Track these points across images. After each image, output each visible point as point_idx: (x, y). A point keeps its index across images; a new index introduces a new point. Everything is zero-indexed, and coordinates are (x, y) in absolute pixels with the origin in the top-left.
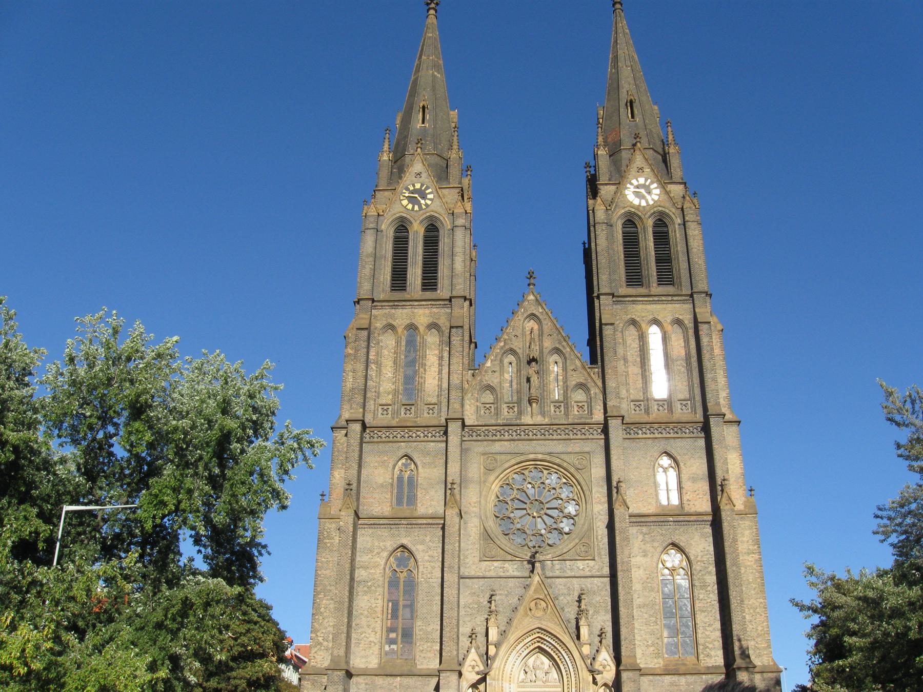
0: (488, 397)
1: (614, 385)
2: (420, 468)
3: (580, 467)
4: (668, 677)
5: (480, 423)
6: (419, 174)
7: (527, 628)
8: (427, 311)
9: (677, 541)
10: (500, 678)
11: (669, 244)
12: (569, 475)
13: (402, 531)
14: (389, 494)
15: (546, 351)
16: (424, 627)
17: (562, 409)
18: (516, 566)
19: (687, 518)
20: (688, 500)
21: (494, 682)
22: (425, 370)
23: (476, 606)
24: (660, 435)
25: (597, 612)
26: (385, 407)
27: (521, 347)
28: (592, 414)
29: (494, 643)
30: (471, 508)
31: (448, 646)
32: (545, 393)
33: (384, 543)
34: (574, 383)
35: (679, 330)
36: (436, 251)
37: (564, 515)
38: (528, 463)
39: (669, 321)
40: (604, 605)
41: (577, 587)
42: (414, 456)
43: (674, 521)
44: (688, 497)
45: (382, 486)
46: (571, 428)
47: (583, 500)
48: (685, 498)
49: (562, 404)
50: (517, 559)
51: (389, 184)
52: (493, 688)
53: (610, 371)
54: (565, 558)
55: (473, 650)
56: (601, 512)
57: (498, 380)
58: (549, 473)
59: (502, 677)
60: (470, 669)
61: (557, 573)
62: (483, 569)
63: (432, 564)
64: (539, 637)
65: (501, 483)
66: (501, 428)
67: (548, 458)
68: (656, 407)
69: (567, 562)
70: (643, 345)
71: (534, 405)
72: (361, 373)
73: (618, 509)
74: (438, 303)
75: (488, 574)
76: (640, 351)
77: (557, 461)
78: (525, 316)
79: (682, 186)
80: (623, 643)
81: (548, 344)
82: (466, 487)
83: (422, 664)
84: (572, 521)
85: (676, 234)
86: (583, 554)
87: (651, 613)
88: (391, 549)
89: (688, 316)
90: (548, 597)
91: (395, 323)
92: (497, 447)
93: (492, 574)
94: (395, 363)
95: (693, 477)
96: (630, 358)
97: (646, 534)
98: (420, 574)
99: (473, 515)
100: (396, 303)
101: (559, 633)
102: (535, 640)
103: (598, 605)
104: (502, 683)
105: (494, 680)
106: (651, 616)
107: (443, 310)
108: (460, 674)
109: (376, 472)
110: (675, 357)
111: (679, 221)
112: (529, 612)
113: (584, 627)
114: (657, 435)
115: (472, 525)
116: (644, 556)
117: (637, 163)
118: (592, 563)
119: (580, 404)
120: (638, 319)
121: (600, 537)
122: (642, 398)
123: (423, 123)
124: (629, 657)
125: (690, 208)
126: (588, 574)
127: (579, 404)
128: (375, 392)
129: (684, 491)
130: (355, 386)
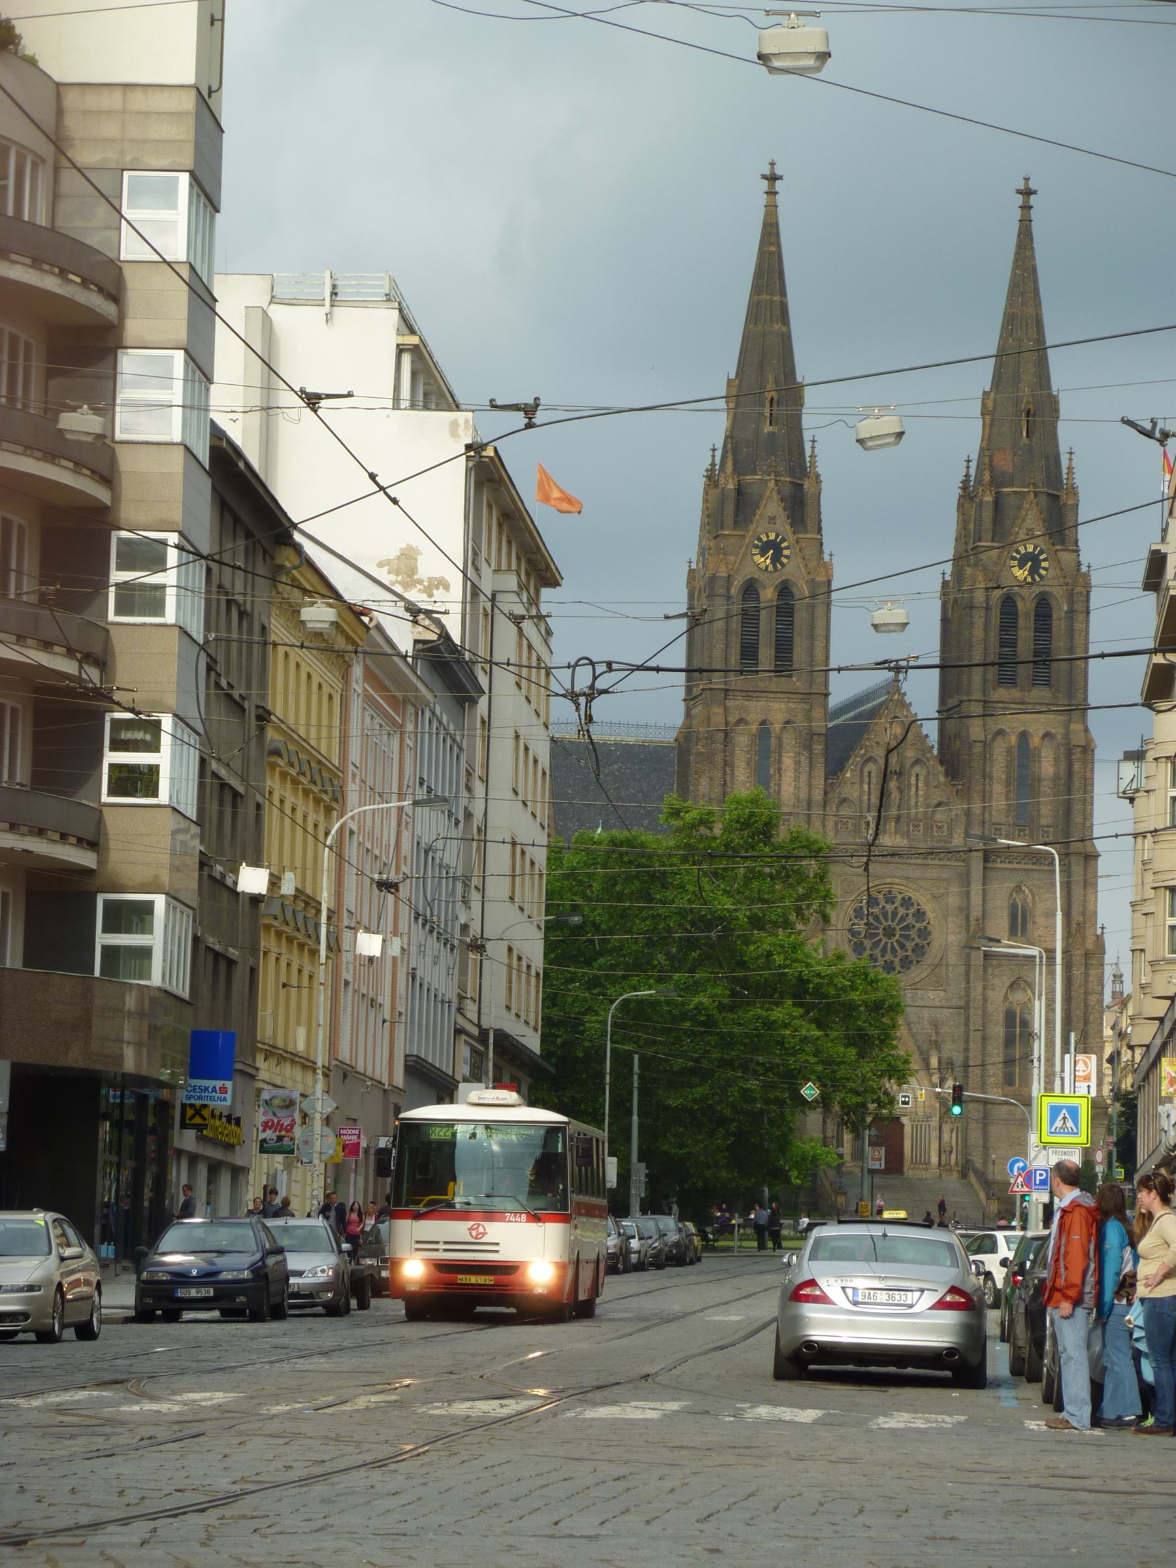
0: (845, 811)
4: (1005, 1106)
5: (838, 842)
6: (772, 519)
8: (783, 706)
11: (1050, 633)
15: (908, 763)
17: (921, 828)
20: (1040, 936)
22: (781, 776)
24: (1017, 866)
28: (951, 838)
34: (936, 802)
36: (792, 623)
39: (1040, 735)
41: (926, 1016)
49: (921, 823)
51: (736, 524)
57: (857, 793)
68: (1017, 832)
72: (718, 782)
74: (794, 696)
76: (1007, 767)
79: (1074, 556)
85: (1059, 625)
89: (1062, 731)
91: (748, 718)
94: (748, 764)
100: (750, 694)
107: (800, 706)
110: (1042, 776)
111: (1065, 608)
114: (1017, 866)
117: (1028, 521)
118: (942, 994)
122: (1003, 822)
123: (771, 424)
125: (1081, 593)
126: (938, 1004)
130: (713, 796)
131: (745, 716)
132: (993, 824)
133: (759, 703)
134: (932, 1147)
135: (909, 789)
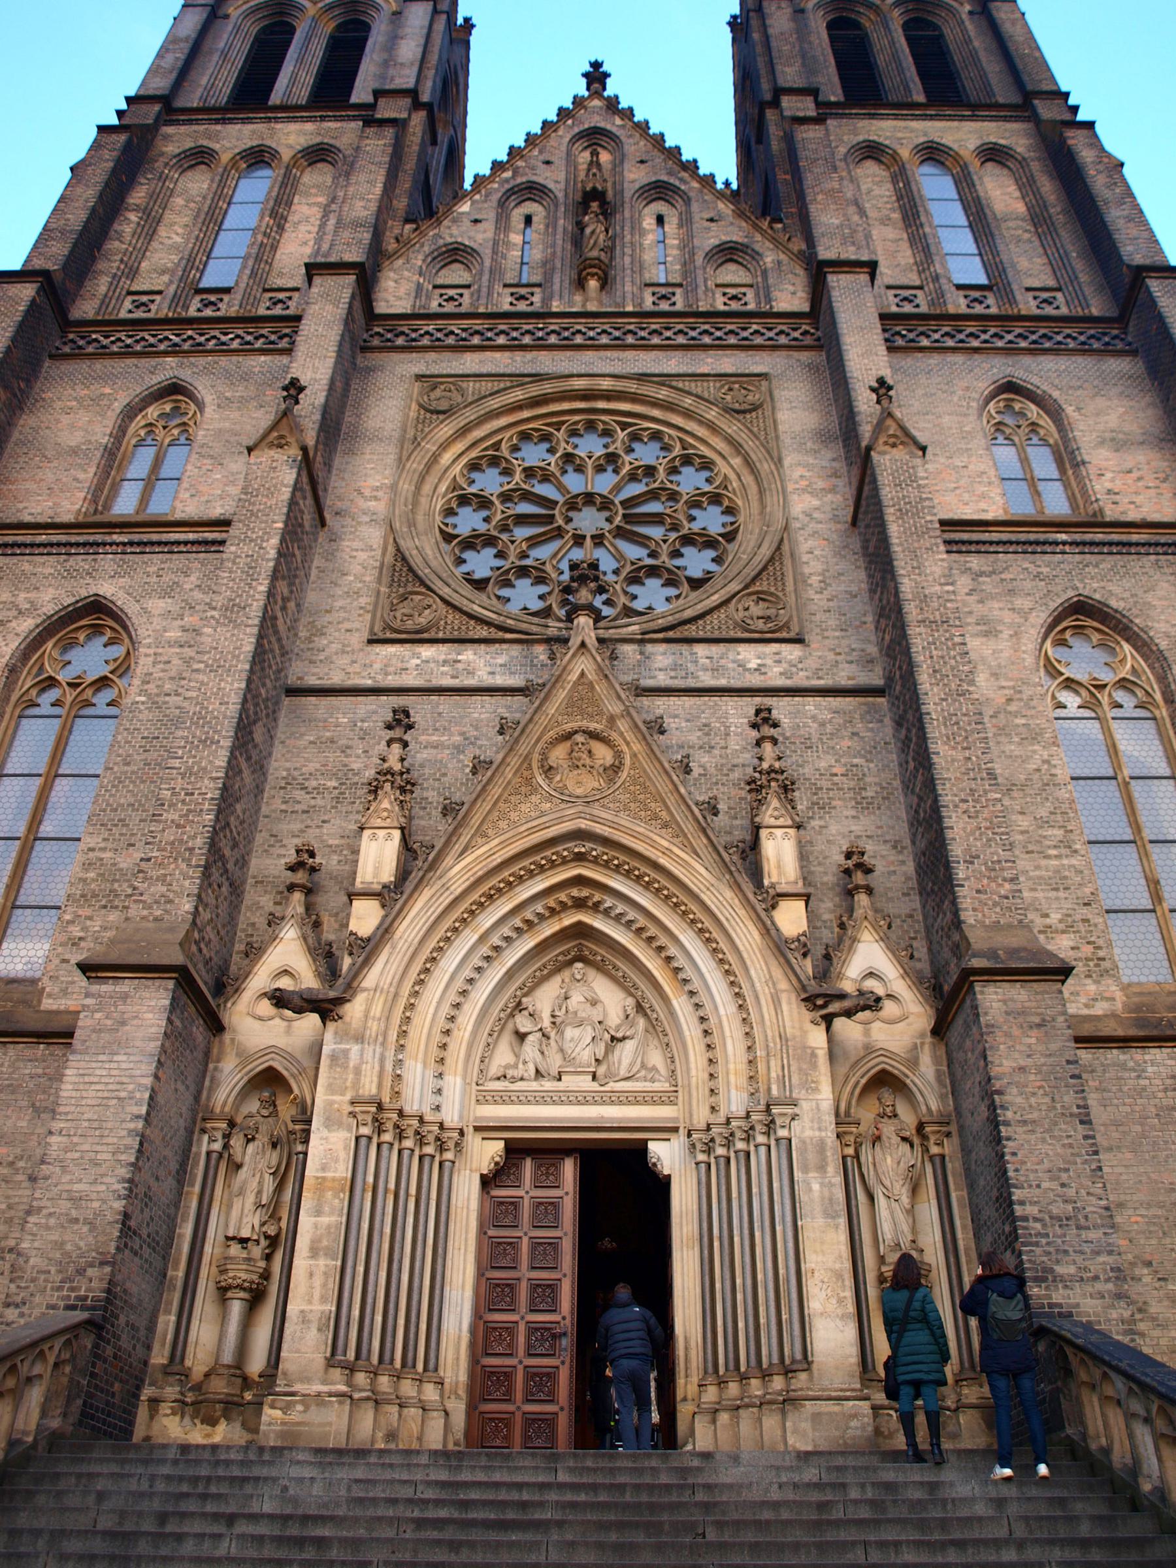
0: (456, 274)
1: (837, 222)
2: (209, 410)
3: (737, 406)
7: (532, 831)
8: (309, 127)
9: (1097, 596)
10: (393, 1035)
12: (701, 432)
13: (107, 562)
14: (93, 470)
15: (629, 190)
16: (107, 855)
18: (500, 661)
19: (1115, 537)
20: (1109, 492)
21: (355, 1049)
22: (281, 229)
23: (334, 783)
25: (823, 807)
26: (144, 299)
27: (562, 176)
29: (377, 887)
30: (362, 504)
31: (162, 879)
32: (627, 260)
33: (33, 595)
34: (714, 242)
35: (1005, 171)
37: (685, 531)
38: (566, 406)
39: (972, 147)
40: (852, 784)
42: (196, 384)
43: (1077, 544)
44: (1108, 485)
45: (74, 451)
46: (706, 327)
47: (753, 489)
48: (1097, 487)
49: (678, 291)
50: (509, 636)
52: (351, 1076)
53: (820, 197)
54: (686, 634)
55: (290, 934)
56: (815, 515)
57: (490, 234)
58: (635, 437)
59: (403, 1034)
60: (266, 1008)
61: (662, 680)
62: (377, 666)
63: (189, 652)
64: (580, 881)
65: (474, 454)
66: (487, 323)
67: (632, 387)
69: (701, 650)
70: (907, 184)
71: (593, 284)
73: (884, 453)
75: (392, 681)
76: (899, 198)
77: (663, 393)
78: (576, 130)
80: (961, 872)
81: (635, 176)
82: (351, 452)
83: (65, 992)
84: (712, 553)
86: (760, 624)
87: (1043, 812)
88: (50, 609)
90: (623, 725)
91: (216, 147)
92: (470, 362)
93: (411, 680)
95: (1113, 440)
96: (872, 213)
97: (982, 574)
98: (136, 682)
99: (367, 519)
101: (666, 852)
102: (563, 897)
103: (825, 784)
104: (399, 1063)
105: (360, 1038)
106: (1043, 823)
108: (216, 1026)
109: (65, 420)
112: (540, 779)
113: (779, 832)
115: (356, 544)
116: (986, 634)
118: (791, 652)
119: (732, 291)
120: (887, 142)
121: (814, 580)
122: (918, 283)
124: (996, 926)
127: (728, 290)
128: (122, 261)
129: (1092, 471)
131: (205, 143)
132: (889, 287)
133: (251, 127)
134: (811, 1260)
135: (636, 228)
